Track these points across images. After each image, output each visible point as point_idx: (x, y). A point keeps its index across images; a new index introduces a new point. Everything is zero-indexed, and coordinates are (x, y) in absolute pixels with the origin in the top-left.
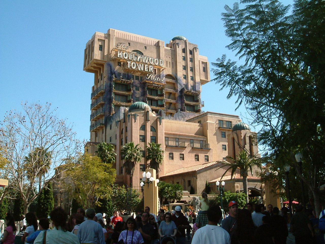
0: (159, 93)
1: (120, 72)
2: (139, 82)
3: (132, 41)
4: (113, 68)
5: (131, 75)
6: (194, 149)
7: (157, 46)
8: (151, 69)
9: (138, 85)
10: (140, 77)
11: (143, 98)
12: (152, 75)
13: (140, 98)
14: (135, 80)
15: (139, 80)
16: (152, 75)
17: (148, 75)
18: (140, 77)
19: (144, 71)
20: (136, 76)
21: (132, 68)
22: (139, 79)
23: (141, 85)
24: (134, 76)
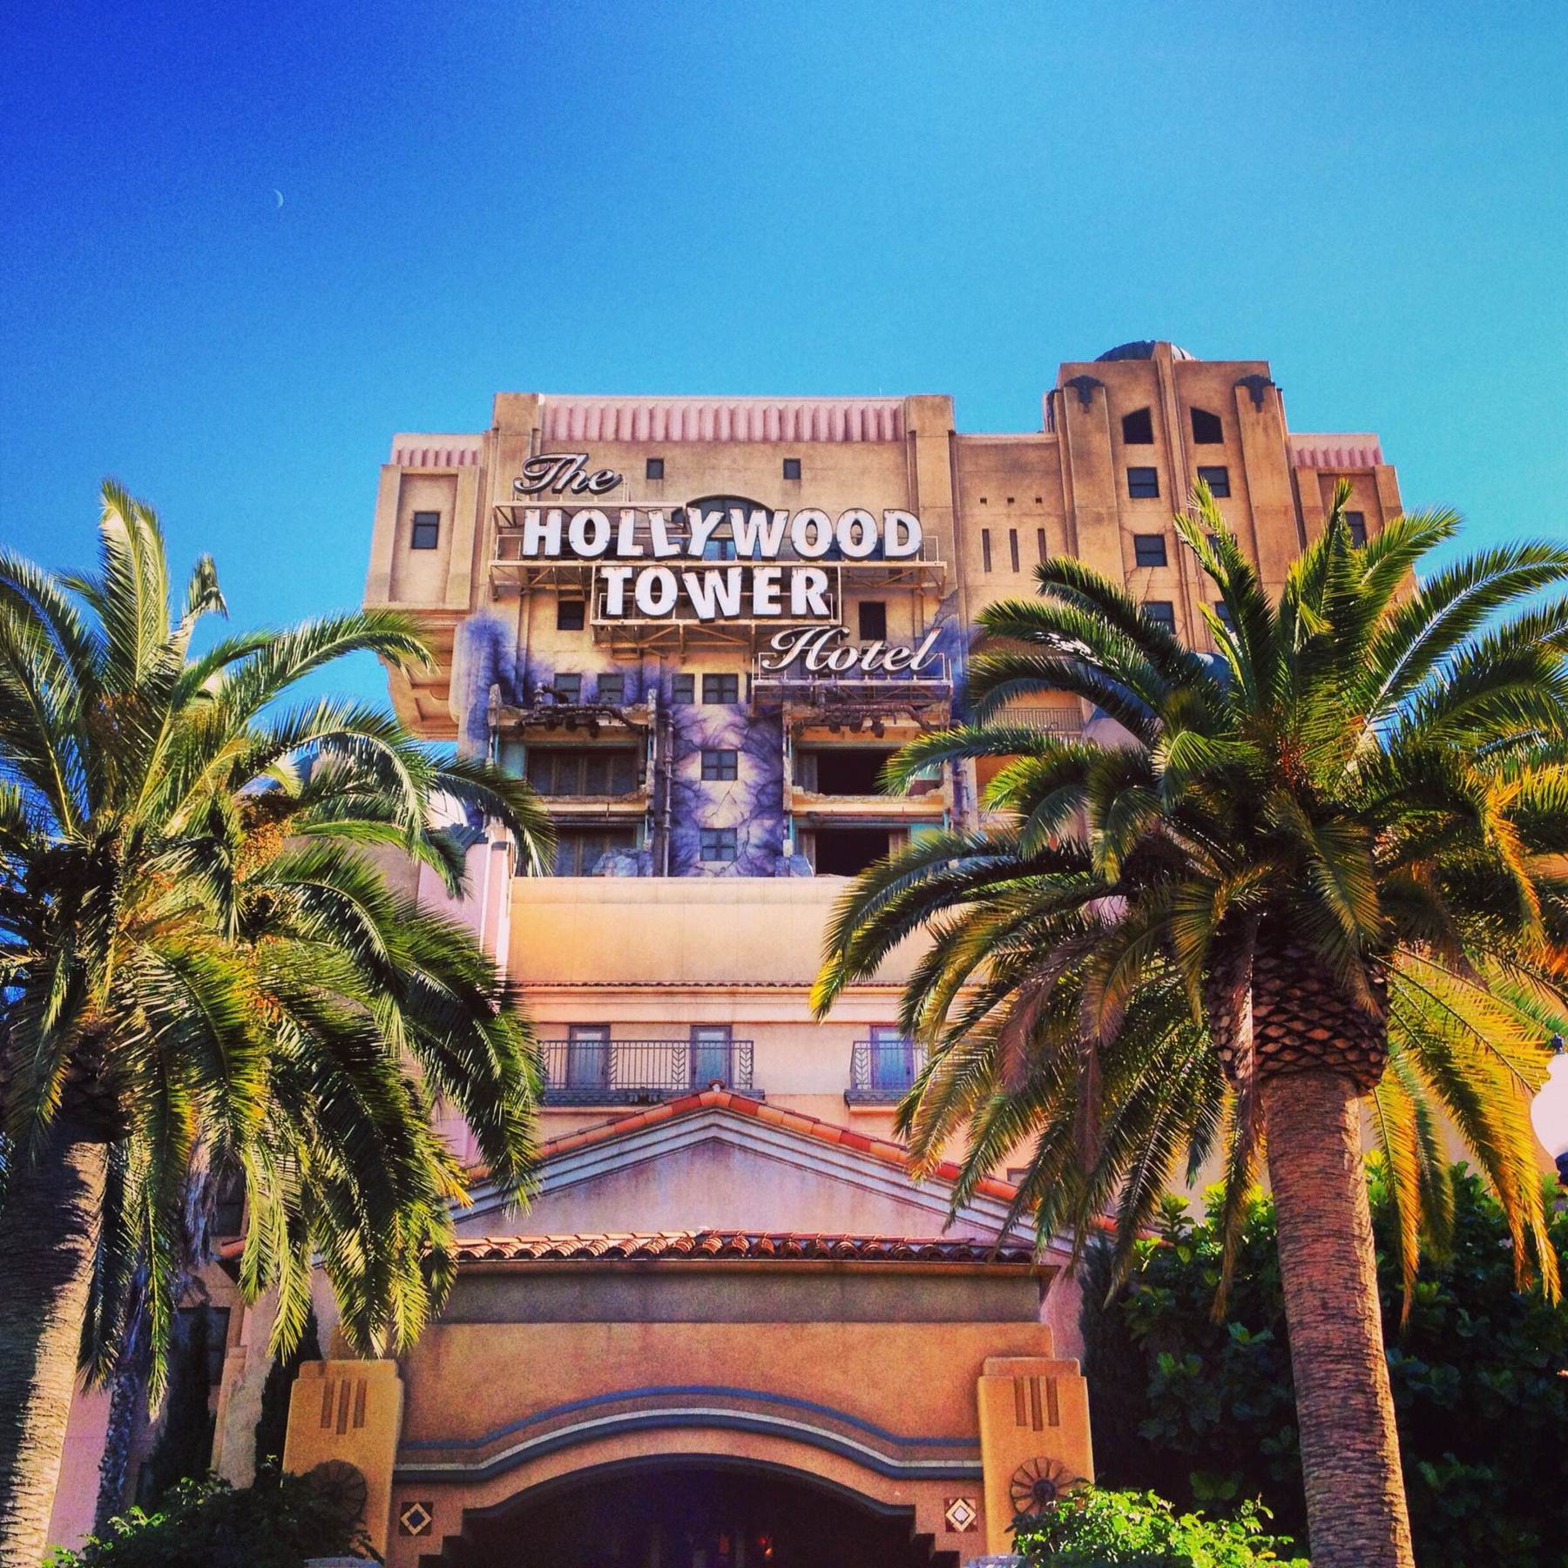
1: (576, 670)
2: (740, 712)
4: (510, 648)
5: (669, 677)
7: (896, 438)
8: (808, 594)
9: (732, 739)
10: (742, 680)
11: (772, 832)
12: (811, 642)
13: (742, 835)
15: (736, 701)
16: (811, 642)
17: (781, 642)
18: (742, 680)
19: (753, 623)
20: (706, 677)
21: (641, 614)
22: (736, 691)
23: (757, 736)
24: (692, 677)
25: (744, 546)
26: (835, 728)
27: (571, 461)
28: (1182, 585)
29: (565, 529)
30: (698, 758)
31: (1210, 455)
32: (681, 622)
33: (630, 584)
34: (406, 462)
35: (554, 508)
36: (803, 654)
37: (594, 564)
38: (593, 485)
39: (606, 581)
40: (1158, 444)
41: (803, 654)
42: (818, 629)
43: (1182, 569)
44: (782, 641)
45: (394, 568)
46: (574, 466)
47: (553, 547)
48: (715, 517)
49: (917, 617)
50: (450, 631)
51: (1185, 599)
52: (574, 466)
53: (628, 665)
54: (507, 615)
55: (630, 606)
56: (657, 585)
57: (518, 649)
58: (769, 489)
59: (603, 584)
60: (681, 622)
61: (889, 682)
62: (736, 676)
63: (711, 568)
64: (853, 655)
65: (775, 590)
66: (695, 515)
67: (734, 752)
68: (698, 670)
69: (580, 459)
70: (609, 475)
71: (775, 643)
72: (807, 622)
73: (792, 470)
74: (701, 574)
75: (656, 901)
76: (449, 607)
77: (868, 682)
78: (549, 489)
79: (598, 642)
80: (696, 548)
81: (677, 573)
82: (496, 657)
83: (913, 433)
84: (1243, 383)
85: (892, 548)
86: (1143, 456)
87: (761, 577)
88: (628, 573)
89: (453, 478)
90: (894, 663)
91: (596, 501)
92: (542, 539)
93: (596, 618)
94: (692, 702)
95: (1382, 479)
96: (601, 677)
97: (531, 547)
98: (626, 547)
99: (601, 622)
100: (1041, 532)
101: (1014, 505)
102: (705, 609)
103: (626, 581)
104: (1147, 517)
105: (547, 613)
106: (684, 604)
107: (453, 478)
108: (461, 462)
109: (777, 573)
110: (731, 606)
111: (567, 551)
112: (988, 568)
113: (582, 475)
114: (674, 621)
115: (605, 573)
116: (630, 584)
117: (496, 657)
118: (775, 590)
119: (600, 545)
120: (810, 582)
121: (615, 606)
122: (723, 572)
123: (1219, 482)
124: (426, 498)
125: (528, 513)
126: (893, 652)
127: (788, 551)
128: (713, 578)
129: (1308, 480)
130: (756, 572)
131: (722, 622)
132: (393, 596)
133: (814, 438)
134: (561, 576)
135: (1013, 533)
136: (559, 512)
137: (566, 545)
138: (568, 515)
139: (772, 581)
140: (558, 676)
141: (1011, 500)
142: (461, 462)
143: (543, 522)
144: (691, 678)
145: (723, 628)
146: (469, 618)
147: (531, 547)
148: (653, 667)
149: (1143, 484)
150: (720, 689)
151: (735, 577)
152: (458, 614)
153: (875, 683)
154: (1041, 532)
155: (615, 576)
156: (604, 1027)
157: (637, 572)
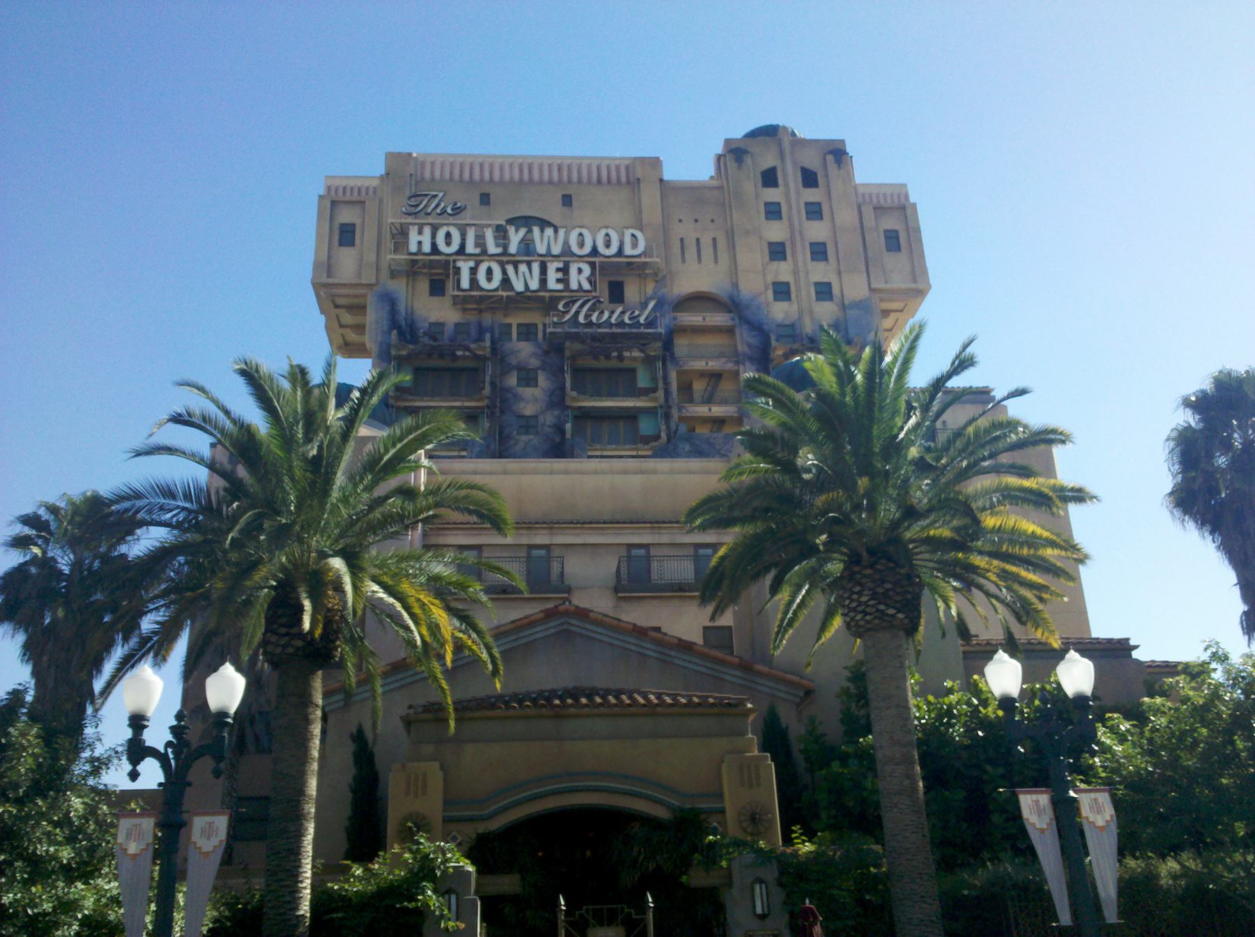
0: (643, 381)
1: (442, 320)
2: (538, 346)
3: (502, 182)
4: (402, 308)
6: (620, 595)
7: (628, 182)
8: (579, 277)
9: (534, 362)
10: (540, 328)
11: (559, 418)
12: (582, 306)
13: (541, 419)
14: (519, 340)
15: (536, 339)
16: (582, 306)
17: (564, 307)
18: (540, 328)
19: (547, 294)
20: (519, 325)
24: (510, 325)
25: (541, 249)
26: (596, 358)
27: (436, 196)
28: (795, 272)
29: (434, 236)
30: (515, 373)
31: (812, 195)
32: (504, 294)
33: (474, 271)
34: (333, 193)
35: (425, 224)
36: (577, 313)
37: (451, 258)
38: (449, 211)
39: (459, 268)
40: (781, 189)
41: (577, 313)
42: (586, 298)
43: (795, 264)
44: (564, 306)
45: (329, 257)
46: (438, 199)
47: (427, 248)
48: (522, 232)
49: (643, 288)
50: (364, 296)
51: (797, 281)
52: (438, 199)
53: (472, 318)
54: (399, 287)
55: (474, 281)
56: (489, 272)
57: (406, 308)
58: (554, 212)
59: (457, 271)
60: (504, 294)
61: (627, 330)
62: (536, 325)
63: (522, 262)
64: (606, 315)
65: (560, 275)
66: (511, 229)
67: (535, 370)
68: (514, 320)
69: (441, 195)
70: (459, 205)
71: (560, 307)
72: (578, 294)
73: (567, 200)
74: (516, 265)
75: (505, 473)
76: (363, 282)
77: (615, 330)
78: (423, 213)
79: (455, 304)
80: (513, 249)
81: (502, 265)
82: (393, 312)
83: (638, 179)
84: (831, 152)
85: (628, 251)
86: (772, 195)
87: (552, 267)
88: (472, 264)
89: (363, 203)
90: (630, 319)
91: (451, 220)
92: (420, 243)
93: (454, 290)
94: (511, 340)
95: (909, 211)
96: (457, 325)
97: (413, 248)
98: (470, 248)
99: (456, 293)
100: (714, 240)
101: (698, 223)
102: (519, 286)
103: (471, 269)
104: (776, 232)
105: (423, 286)
106: (506, 282)
107: (363, 203)
108: (367, 194)
109: (561, 265)
110: (534, 285)
111: (435, 249)
112: (684, 261)
113: (442, 205)
114: (501, 293)
115: (459, 264)
116: (474, 271)
117: (393, 312)
118: (560, 275)
119: (455, 247)
120: (580, 271)
121: (465, 284)
122: (529, 264)
123: (814, 211)
124: (347, 216)
125: (411, 227)
126: (629, 313)
127: (567, 251)
128: (523, 268)
129: (868, 213)
130: (549, 265)
131: (529, 294)
132: (329, 275)
133: (580, 181)
134: (432, 265)
135: (698, 240)
136: (429, 226)
137: (434, 246)
138: (435, 229)
139: (558, 270)
140: (430, 324)
141: (696, 221)
142: (367, 194)
143: (420, 233)
144: (510, 325)
145: (529, 298)
146: (375, 288)
147: (413, 248)
148: (487, 319)
149: (773, 212)
150: (527, 332)
151: (536, 267)
152: (370, 286)
153: (619, 330)
154: (714, 240)
155: (465, 266)
156: (478, 548)
157: (478, 264)
